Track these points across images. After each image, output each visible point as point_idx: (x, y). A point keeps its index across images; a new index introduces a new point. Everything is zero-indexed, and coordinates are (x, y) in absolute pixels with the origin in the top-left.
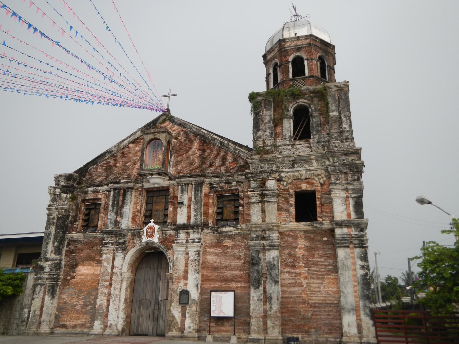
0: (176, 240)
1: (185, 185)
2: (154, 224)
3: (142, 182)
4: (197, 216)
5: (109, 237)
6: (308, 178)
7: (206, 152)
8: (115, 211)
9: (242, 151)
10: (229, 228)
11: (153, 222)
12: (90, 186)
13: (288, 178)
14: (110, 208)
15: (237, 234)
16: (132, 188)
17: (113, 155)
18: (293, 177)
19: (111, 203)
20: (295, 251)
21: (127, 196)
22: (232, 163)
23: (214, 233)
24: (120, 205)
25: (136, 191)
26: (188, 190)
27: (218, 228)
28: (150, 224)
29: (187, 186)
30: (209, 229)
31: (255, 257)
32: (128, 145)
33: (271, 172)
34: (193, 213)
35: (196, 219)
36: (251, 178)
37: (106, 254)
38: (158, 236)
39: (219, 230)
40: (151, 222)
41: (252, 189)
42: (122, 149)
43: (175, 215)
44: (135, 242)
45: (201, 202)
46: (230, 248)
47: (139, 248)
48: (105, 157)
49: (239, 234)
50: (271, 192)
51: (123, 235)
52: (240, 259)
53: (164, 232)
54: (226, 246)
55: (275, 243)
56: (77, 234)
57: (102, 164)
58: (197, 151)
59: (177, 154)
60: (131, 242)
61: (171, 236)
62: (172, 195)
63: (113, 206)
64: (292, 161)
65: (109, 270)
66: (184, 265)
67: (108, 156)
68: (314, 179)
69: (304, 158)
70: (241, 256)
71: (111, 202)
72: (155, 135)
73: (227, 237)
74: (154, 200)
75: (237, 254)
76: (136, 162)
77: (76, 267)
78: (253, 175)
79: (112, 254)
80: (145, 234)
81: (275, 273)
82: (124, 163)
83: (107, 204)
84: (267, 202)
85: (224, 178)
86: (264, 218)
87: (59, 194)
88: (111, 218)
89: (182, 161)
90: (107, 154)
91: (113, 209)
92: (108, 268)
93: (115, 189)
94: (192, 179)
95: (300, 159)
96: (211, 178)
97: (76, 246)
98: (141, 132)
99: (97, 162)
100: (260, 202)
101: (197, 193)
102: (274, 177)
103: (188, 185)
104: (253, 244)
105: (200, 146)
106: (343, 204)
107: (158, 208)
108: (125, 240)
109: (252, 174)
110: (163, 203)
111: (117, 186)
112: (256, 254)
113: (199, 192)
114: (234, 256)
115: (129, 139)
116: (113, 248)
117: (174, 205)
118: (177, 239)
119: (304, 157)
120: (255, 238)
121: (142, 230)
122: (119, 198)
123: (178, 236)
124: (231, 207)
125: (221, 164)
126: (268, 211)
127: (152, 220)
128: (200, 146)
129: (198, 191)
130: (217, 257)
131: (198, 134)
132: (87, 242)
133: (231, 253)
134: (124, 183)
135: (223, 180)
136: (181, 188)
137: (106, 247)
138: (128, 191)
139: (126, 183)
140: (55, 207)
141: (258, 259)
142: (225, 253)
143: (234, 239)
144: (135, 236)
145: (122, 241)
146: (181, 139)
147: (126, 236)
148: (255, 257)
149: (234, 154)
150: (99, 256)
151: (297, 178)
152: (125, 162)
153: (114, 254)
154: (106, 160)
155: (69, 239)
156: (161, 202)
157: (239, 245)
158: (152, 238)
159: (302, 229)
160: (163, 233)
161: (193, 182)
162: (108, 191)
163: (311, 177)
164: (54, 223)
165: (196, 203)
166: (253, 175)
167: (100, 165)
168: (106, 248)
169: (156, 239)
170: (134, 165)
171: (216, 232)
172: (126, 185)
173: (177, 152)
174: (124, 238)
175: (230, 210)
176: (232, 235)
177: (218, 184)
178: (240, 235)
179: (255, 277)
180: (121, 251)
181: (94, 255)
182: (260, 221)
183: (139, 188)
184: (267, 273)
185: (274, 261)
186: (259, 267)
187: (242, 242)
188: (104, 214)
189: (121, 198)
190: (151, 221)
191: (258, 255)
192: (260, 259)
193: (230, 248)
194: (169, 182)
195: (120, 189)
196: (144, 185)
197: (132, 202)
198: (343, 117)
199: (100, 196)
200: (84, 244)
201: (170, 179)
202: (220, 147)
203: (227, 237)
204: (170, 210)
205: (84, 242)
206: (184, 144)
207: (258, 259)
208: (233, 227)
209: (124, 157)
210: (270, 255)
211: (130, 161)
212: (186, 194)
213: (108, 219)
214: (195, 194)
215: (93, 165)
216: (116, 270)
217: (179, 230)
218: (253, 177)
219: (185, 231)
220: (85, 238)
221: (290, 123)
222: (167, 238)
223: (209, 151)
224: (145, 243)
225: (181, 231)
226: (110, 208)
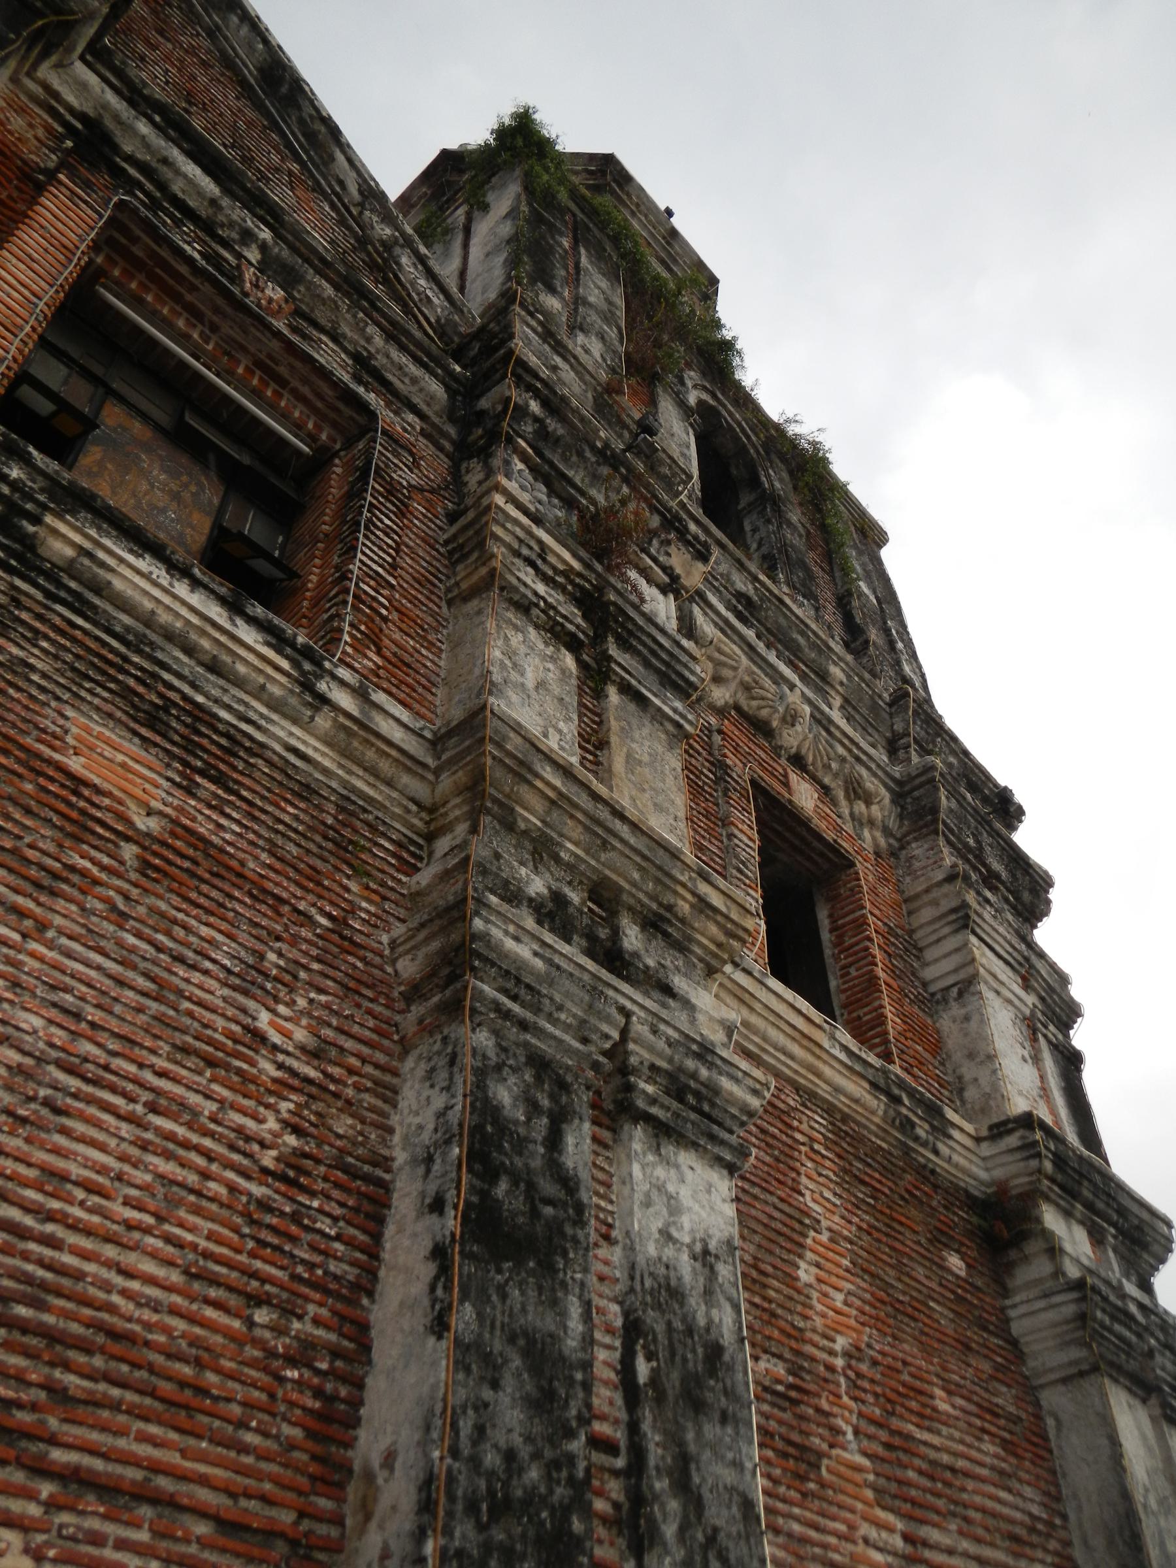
13: (718, 664)
18: (747, 688)
20: (791, 1280)
31: (521, 1144)
36: (529, 428)
46: (129, 851)
52: (246, 1083)
55: (726, 1083)
73: (126, 693)
78: (552, 424)
81: (728, 1476)
95: (779, 628)
96: (134, 96)
102: (678, 570)
104: (524, 951)
112: (533, 1108)
114: (162, 991)
135: (247, 236)
141: (548, 1187)
143: (219, 780)
148: (521, 1144)
151: (764, 713)
157: (260, 894)
159: (823, 1090)
163: (819, 774)
166: (552, 424)
176: (200, 716)
179: (510, 1456)
184: (656, 1453)
185: (708, 1293)
186: (555, 1304)
187: (312, 879)
191: (554, 1141)
192: (568, 1183)
193: (129, 851)
202: (243, 83)
203: (126, 693)
207: (548, 1187)
210: (674, 1208)
218: (543, 433)
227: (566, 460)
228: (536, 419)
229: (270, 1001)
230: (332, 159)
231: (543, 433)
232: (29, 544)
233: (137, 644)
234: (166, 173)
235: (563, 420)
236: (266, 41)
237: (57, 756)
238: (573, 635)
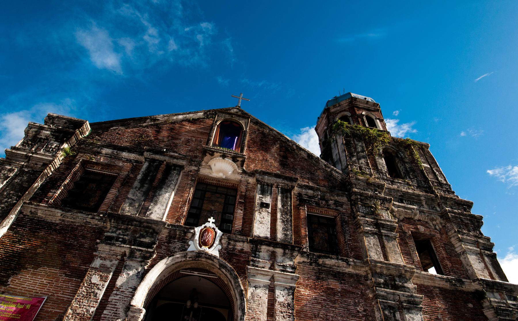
0: (253, 260)
1: (268, 185)
2: (213, 226)
3: (199, 164)
4: (287, 231)
5: (120, 229)
6: (421, 221)
7: (288, 159)
8: (144, 189)
9: (335, 171)
10: (336, 261)
11: (213, 223)
12: (108, 146)
14: (136, 184)
15: (346, 273)
16: (182, 167)
17: (157, 125)
19: (139, 177)
21: (171, 175)
22: (322, 180)
23: (311, 264)
24: (155, 183)
25: (184, 174)
26: (271, 192)
27: (319, 257)
28: (207, 224)
29: (270, 188)
30: (305, 255)
32: (181, 122)
33: (384, 200)
34: (280, 226)
35: (286, 235)
37: (105, 259)
38: (220, 247)
39: (321, 261)
40: (209, 222)
41: (362, 214)
42: (172, 123)
43: (248, 222)
44: (172, 249)
45: (291, 212)
46: (339, 294)
47: (179, 260)
48: (145, 122)
49: (349, 274)
50: (389, 223)
51: (151, 231)
53: (232, 242)
54: (332, 289)
56: (49, 209)
57: (135, 130)
58: (276, 156)
59: (250, 151)
60: (163, 247)
61: (243, 253)
62: (243, 194)
63: (143, 182)
64: (400, 196)
65: (101, 294)
66: (266, 311)
67: (149, 122)
68: (429, 224)
69: (414, 197)
70: (358, 312)
71: (140, 175)
72: (232, 117)
73: (332, 274)
74: (206, 196)
75: (352, 308)
76: (189, 142)
77: (13, 274)
78: (362, 198)
79: (116, 262)
80: (197, 237)
82: (170, 138)
83: (128, 179)
84: (385, 236)
85: (319, 192)
86: (386, 257)
87: (44, 139)
88: (133, 198)
89: (256, 159)
90: (148, 120)
91: (142, 186)
92: (98, 289)
93: (152, 161)
94: (279, 180)
97: (34, 232)
98: (204, 114)
99: (129, 124)
100: (376, 234)
101: (285, 199)
103: (272, 187)
105: (280, 151)
106: (480, 261)
107: (213, 208)
108: (153, 239)
109: (361, 196)
110: (220, 204)
111: (157, 157)
113: (289, 199)
115: (186, 115)
116: (123, 250)
117: (245, 209)
118: (255, 259)
119: (413, 195)
120: (383, 284)
121: (192, 231)
122: (156, 175)
123: (256, 254)
124: (323, 233)
125: (309, 178)
126: (390, 248)
127: (212, 220)
128: (280, 151)
129: (287, 198)
130: (319, 307)
131: (279, 139)
132: (63, 229)
133: (341, 303)
134: (171, 156)
135: (318, 195)
136: (261, 187)
137: (110, 244)
138: (175, 169)
139: (175, 158)
140: (25, 153)
142: (331, 301)
143: (344, 280)
144: (174, 238)
145: (147, 240)
146: (256, 137)
147: (157, 233)
149: (324, 172)
150: (79, 261)
151: (410, 216)
152: (172, 137)
153: (122, 261)
154: (144, 127)
155: (25, 216)
156: (217, 202)
158: (209, 248)
160: (229, 244)
161: (281, 184)
162: (137, 161)
164: (6, 178)
165: (284, 213)
166: (362, 198)
167: (131, 130)
168: (107, 247)
169: (214, 251)
170: (186, 145)
171: (315, 263)
172: (175, 160)
173: (251, 149)
174: (152, 237)
175: (323, 237)
176: (339, 272)
177: (310, 197)
178: (351, 275)
180: (139, 259)
181: (69, 256)
182: (382, 260)
183: (191, 171)
187: (356, 288)
188: (119, 191)
189: (159, 176)
190: (209, 220)
194: (241, 175)
195: (161, 162)
196: (201, 170)
197: (177, 187)
198: (435, 171)
199: (121, 164)
200: (55, 230)
201: (244, 172)
203: (332, 274)
204: (239, 213)
205: (58, 227)
206: (259, 143)
208: (343, 260)
209: (172, 132)
211: (180, 139)
212: (269, 197)
213: (128, 198)
214: (282, 201)
215: (121, 126)
216: (117, 297)
217: (262, 244)
219: (271, 249)
220: (63, 221)
221: (382, 160)
222: (236, 255)
223: (292, 160)
224: (194, 254)
225: (264, 248)
226: (136, 184)
227: (366, 201)
228: (360, 198)
229: (358, 306)
230: (320, 163)
231: (361, 201)
232: (318, 263)
233: (330, 268)
234: (308, 194)
235: (363, 196)
236: (306, 151)
237: (329, 287)
238: (376, 233)
